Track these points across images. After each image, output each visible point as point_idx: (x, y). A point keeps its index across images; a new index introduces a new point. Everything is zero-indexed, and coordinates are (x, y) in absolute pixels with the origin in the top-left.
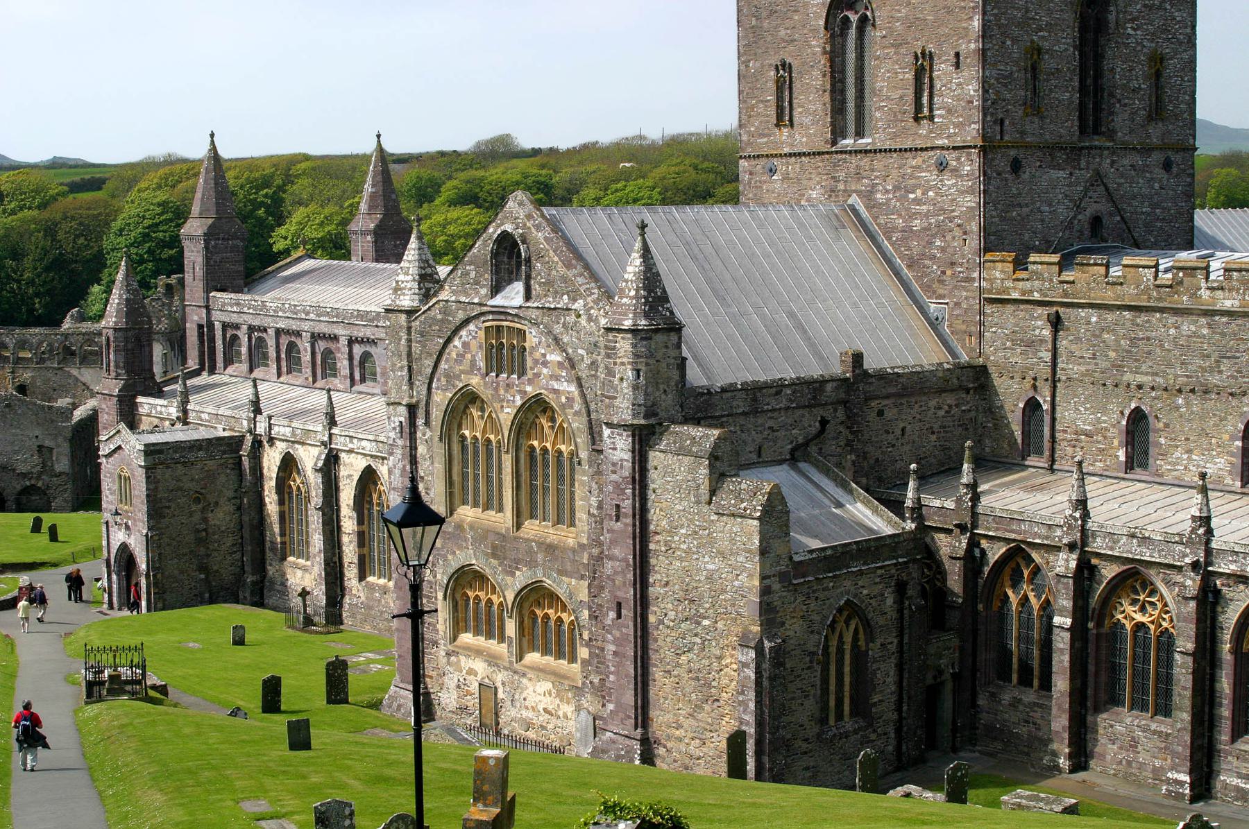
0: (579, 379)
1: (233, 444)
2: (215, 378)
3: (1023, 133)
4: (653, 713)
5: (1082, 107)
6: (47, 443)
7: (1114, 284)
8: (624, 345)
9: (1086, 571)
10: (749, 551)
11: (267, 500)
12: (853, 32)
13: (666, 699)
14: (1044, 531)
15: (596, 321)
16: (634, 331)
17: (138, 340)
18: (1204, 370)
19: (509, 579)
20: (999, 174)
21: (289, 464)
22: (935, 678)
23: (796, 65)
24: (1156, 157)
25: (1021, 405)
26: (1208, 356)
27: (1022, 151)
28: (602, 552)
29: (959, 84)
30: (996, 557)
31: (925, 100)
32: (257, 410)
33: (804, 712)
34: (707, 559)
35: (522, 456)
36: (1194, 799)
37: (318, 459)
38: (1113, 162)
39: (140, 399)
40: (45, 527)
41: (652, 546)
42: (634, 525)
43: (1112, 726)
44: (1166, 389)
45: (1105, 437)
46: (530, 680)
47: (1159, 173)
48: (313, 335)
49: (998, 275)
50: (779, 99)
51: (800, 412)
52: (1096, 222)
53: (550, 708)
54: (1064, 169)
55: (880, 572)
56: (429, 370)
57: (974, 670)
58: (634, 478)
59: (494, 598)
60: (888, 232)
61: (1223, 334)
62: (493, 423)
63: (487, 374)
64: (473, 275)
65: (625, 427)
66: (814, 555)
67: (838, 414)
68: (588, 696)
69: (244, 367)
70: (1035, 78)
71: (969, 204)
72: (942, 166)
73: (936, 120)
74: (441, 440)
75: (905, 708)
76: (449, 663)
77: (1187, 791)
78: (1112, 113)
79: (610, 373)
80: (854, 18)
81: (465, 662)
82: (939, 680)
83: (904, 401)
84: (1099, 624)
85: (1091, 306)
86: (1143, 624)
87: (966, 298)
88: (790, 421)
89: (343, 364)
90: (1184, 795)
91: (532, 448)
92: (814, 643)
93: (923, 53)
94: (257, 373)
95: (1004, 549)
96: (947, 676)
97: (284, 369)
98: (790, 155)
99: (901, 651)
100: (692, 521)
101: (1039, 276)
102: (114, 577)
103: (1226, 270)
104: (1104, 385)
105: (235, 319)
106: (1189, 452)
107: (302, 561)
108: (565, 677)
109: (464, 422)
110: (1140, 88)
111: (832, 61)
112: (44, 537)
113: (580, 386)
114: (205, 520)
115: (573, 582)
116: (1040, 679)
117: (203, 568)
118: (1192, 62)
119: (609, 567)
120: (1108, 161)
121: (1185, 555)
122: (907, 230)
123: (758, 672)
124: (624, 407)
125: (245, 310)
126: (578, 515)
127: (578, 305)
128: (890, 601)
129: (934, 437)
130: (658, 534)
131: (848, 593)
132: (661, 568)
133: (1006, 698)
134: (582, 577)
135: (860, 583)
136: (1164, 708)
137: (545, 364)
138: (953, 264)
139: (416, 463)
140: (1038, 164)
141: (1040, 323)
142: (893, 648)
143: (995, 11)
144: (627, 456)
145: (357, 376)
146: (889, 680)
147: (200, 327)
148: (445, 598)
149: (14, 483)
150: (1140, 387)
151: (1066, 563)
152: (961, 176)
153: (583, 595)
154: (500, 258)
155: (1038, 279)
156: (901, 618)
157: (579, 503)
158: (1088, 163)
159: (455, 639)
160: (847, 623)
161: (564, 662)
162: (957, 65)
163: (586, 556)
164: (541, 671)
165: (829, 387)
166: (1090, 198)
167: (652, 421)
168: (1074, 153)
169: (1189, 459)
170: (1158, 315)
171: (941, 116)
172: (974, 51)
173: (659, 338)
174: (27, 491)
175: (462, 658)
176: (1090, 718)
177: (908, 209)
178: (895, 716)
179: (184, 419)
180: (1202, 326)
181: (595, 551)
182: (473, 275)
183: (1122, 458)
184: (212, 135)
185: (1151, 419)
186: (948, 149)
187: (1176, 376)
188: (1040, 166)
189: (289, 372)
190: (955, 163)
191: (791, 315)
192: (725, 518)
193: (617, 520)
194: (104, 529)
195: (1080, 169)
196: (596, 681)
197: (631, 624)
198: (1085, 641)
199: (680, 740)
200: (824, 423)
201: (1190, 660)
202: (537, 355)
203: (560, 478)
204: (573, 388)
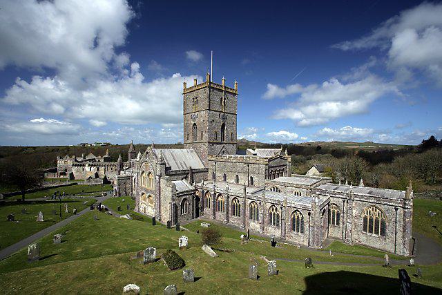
124: (158, 173)
132: (162, 193)
151: (213, 193)
168: (221, 144)
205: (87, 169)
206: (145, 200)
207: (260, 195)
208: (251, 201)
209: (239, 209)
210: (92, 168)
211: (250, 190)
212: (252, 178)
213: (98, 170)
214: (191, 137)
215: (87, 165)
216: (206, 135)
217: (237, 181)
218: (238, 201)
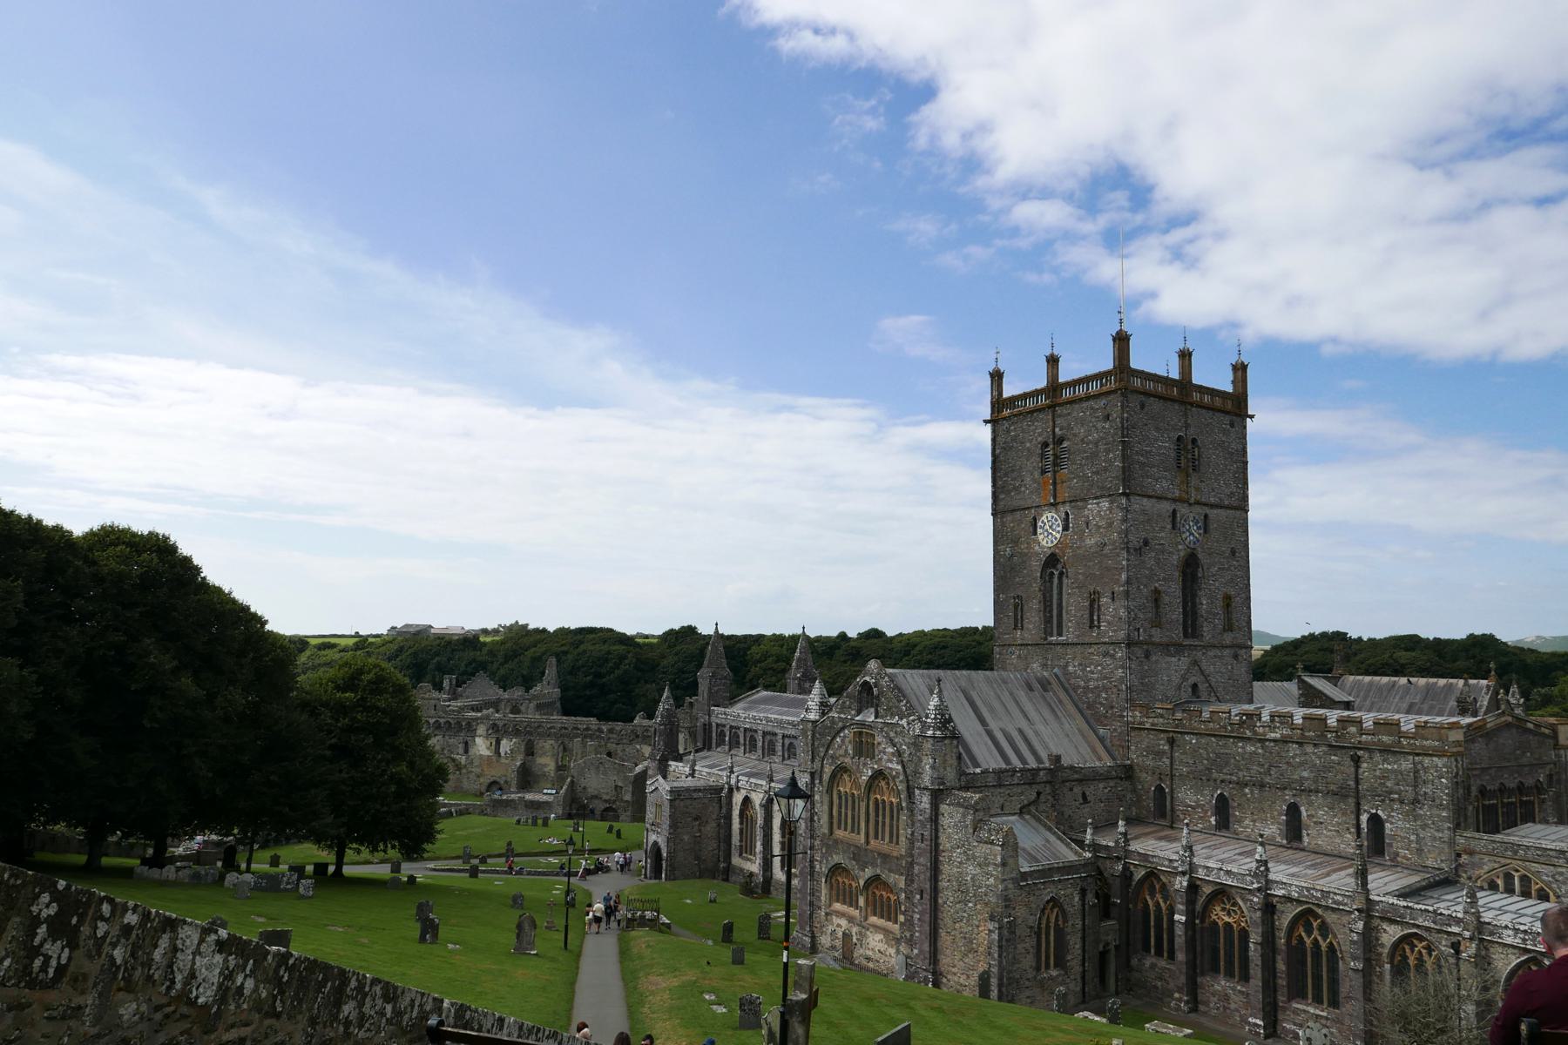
0: (902, 761)
1: (719, 790)
2: (710, 753)
3: (1151, 636)
4: (941, 957)
5: (1185, 621)
6: (620, 784)
7: (1204, 722)
8: (928, 745)
9: (1193, 887)
10: (995, 864)
11: (734, 821)
12: (1056, 581)
13: (947, 948)
14: (1167, 863)
15: (914, 730)
16: (934, 737)
17: (671, 730)
18: (1260, 773)
19: (861, 873)
20: (1137, 658)
21: (747, 800)
22: (1104, 947)
23: (1024, 596)
24: (1227, 652)
25: (1153, 789)
26: (1263, 765)
27: (1150, 646)
28: (913, 860)
30: (1140, 876)
31: (1095, 618)
32: (732, 772)
33: (1028, 962)
34: (971, 868)
35: (871, 803)
36: (1266, 1037)
37: (763, 800)
38: (1204, 653)
39: (670, 763)
40: (614, 831)
41: (941, 859)
42: (931, 846)
43: (1213, 986)
44: (1238, 783)
45: (1202, 809)
46: (871, 932)
48: (764, 732)
49: (1137, 713)
50: (1016, 615)
51: (1027, 786)
52: (1195, 686)
53: (882, 950)
55: (1071, 881)
56: (822, 754)
57: (1128, 944)
58: (931, 819)
59: (853, 884)
60: (1075, 689)
61: (1271, 753)
62: (856, 784)
63: (853, 758)
64: (848, 703)
65: (926, 788)
66: (1032, 869)
67: (1047, 789)
68: (903, 944)
69: (727, 747)
70: (1157, 607)
72: (1106, 654)
74: (827, 792)
75: (1086, 965)
76: (827, 920)
77: (1262, 1031)
78: (1202, 627)
79: (920, 760)
80: (1056, 573)
81: (836, 920)
82: (1107, 948)
83: (1084, 782)
84: (1202, 921)
85: (1193, 734)
86: (1229, 923)
87: (1120, 726)
88: (1020, 791)
89: (779, 748)
90: (1261, 1033)
91: (876, 798)
92: (1032, 920)
93: (1094, 592)
94: (732, 752)
95: (1143, 873)
96: (1112, 947)
97: (748, 750)
98: (1022, 645)
99: (1084, 930)
100: (963, 845)
101: (1162, 716)
102: (649, 861)
103: (1272, 716)
104: (1201, 779)
105: (723, 722)
106: (1254, 821)
107: (752, 857)
108: (892, 933)
109: (840, 784)
110: (1218, 613)
111: (1044, 595)
112: (613, 836)
113: (903, 767)
114: (700, 831)
115: (897, 877)
116: (1168, 952)
117: (698, 858)
118: (1249, 598)
119: (916, 869)
121: (1253, 883)
122: (1086, 688)
123: (1000, 934)
124: (926, 780)
125: (729, 717)
126: (900, 839)
127: (904, 722)
128: (1077, 899)
129: (1102, 805)
130: (944, 851)
131: (1052, 892)
132: (946, 869)
133: (1148, 963)
134: (902, 874)
135: (1059, 887)
136: (1245, 977)
137: (884, 753)
138: (1112, 707)
139: (814, 804)
141: (1162, 742)
142: (1079, 926)
144: (928, 806)
145: (786, 756)
146: (1077, 946)
147: (705, 725)
148: (826, 882)
149: (601, 805)
150: (1222, 781)
151: (1181, 883)
152: (1116, 659)
153: (902, 885)
154: (862, 695)
155: (1161, 717)
156: (1084, 909)
157: (901, 831)
159: (830, 906)
160: (1052, 909)
161: (890, 924)
162: (1113, 599)
163: (904, 862)
164: (877, 928)
165: (1042, 773)
167: (941, 787)
169: (1254, 825)
170: (1231, 740)
173: (947, 741)
174: (606, 810)
175: (834, 917)
176: (1199, 980)
177: (1086, 676)
178: (1081, 969)
179: (692, 775)
180: (1257, 748)
181: (910, 860)
182: (848, 703)
183: (1214, 823)
184: (717, 624)
185: (1230, 801)
186: (1108, 643)
187: (1244, 776)
189: (750, 752)
190: (1112, 652)
191: (1021, 731)
192: (981, 845)
193: (922, 842)
194: (645, 833)
196: (908, 935)
197: (928, 903)
198: (1194, 931)
199: (955, 974)
200: (1039, 794)
201: (1259, 947)
202: (880, 748)
203: (892, 817)
204: (899, 767)
205: (482, 746)
206: (849, 898)
207: (1452, 904)
208: (1390, 934)
209: (1333, 969)
210: (506, 745)
211: (1384, 884)
212: (1376, 821)
213: (530, 751)
214: (1033, 620)
215: (481, 730)
216: (1113, 611)
217: (1294, 829)
218: (1325, 929)
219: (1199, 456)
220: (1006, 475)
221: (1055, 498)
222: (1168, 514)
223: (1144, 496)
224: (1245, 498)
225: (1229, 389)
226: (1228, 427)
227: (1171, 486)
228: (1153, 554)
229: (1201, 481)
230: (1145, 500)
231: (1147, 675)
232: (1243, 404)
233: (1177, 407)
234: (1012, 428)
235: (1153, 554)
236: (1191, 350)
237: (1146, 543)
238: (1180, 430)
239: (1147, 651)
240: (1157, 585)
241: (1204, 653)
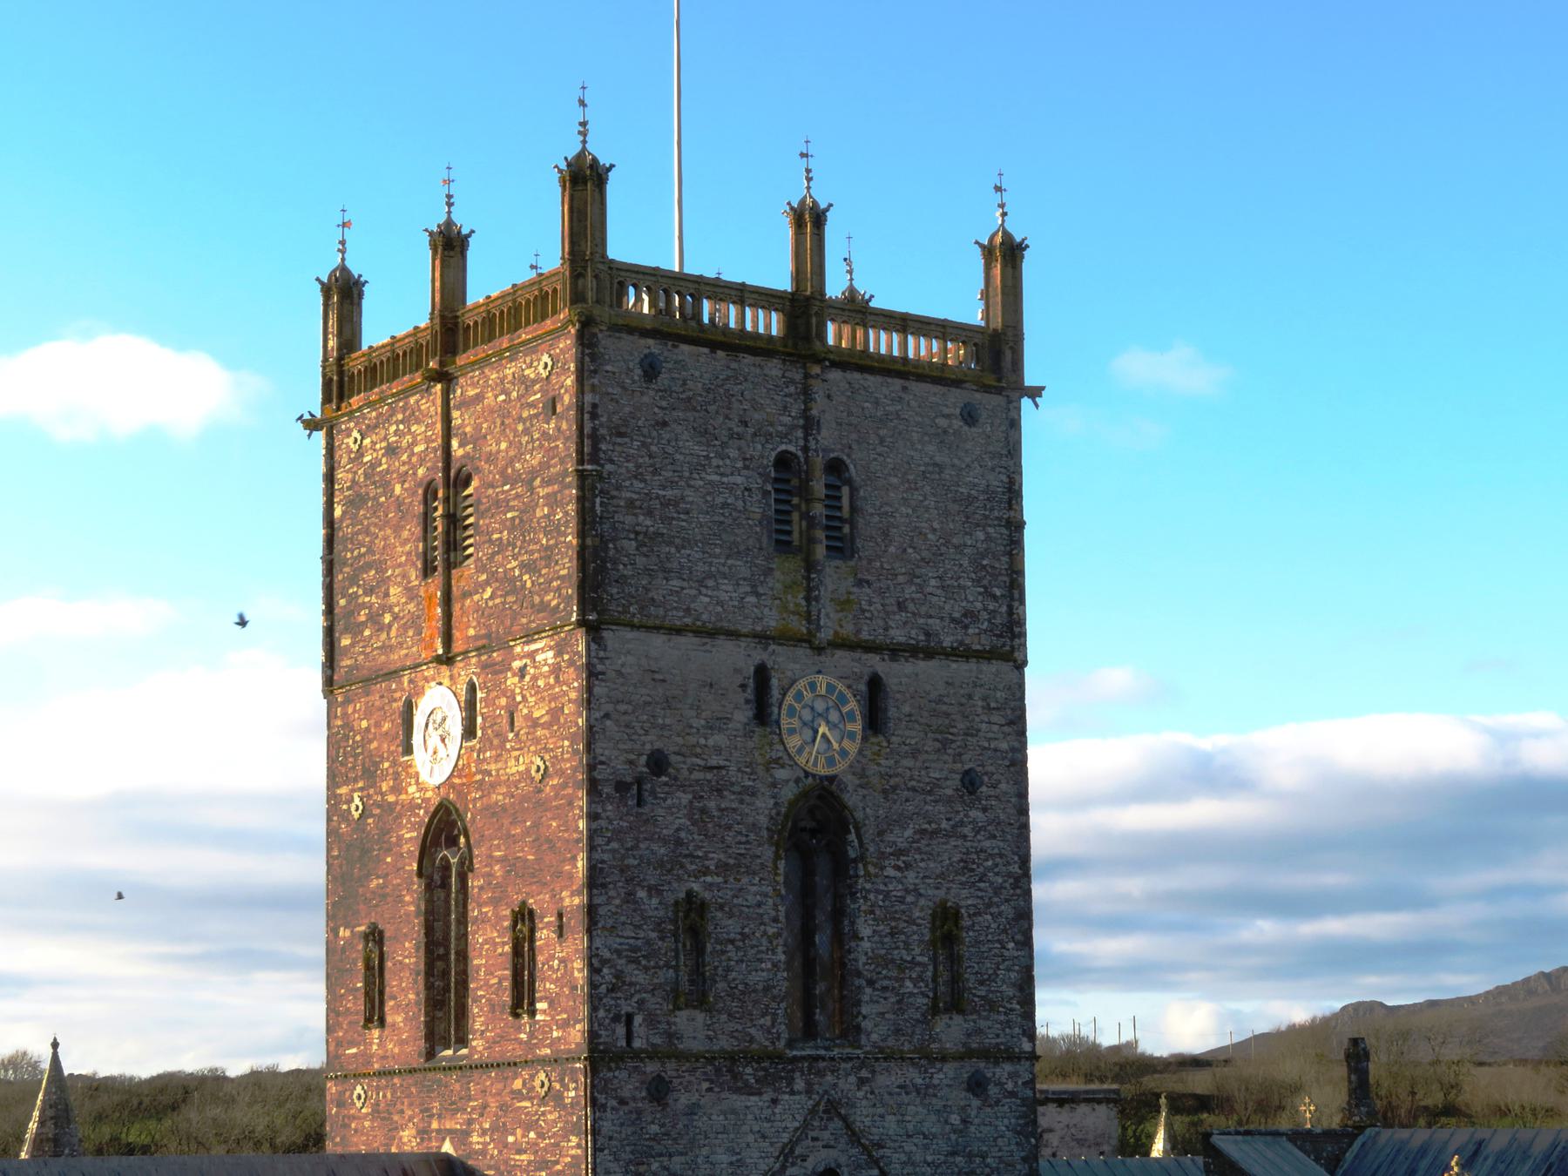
27: (671, 1065)
29: (562, 961)
38: (862, 1082)
47: (959, 1097)
54: (760, 1094)
71: (573, 1152)
73: (538, 1017)
78: (858, 1003)
98: (380, 1074)
110: (913, 963)
120: (852, 1079)
140: (706, 1085)
143: (614, 845)
158: (809, 1084)
166: (815, 1139)
171: (544, 1012)
172: (578, 906)
188: (709, 1090)
195: (792, 1093)
219: (854, 509)
220: (353, 580)
221: (448, 640)
222: (739, 680)
223: (657, 628)
224: (1014, 628)
225: (972, 313)
226: (957, 423)
227: (752, 599)
228: (685, 798)
229: (860, 583)
230: (658, 641)
231: (658, 1148)
232: (1008, 355)
233: (776, 372)
234: (367, 441)
235: (685, 798)
236: (823, 206)
237: (658, 763)
238: (784, 437)
239: (659, 1079)
240: (696, 887)
241: (862, 1082)
